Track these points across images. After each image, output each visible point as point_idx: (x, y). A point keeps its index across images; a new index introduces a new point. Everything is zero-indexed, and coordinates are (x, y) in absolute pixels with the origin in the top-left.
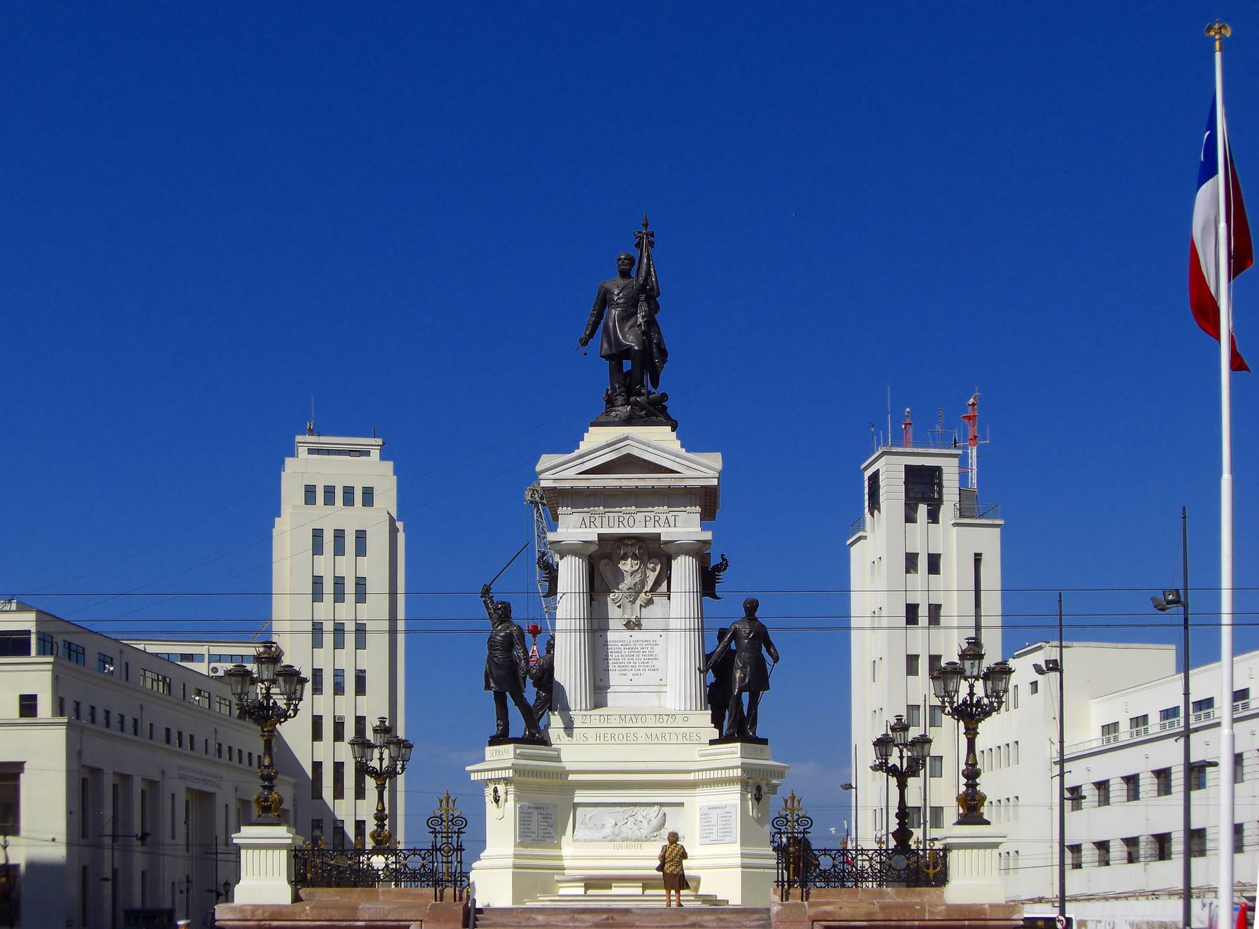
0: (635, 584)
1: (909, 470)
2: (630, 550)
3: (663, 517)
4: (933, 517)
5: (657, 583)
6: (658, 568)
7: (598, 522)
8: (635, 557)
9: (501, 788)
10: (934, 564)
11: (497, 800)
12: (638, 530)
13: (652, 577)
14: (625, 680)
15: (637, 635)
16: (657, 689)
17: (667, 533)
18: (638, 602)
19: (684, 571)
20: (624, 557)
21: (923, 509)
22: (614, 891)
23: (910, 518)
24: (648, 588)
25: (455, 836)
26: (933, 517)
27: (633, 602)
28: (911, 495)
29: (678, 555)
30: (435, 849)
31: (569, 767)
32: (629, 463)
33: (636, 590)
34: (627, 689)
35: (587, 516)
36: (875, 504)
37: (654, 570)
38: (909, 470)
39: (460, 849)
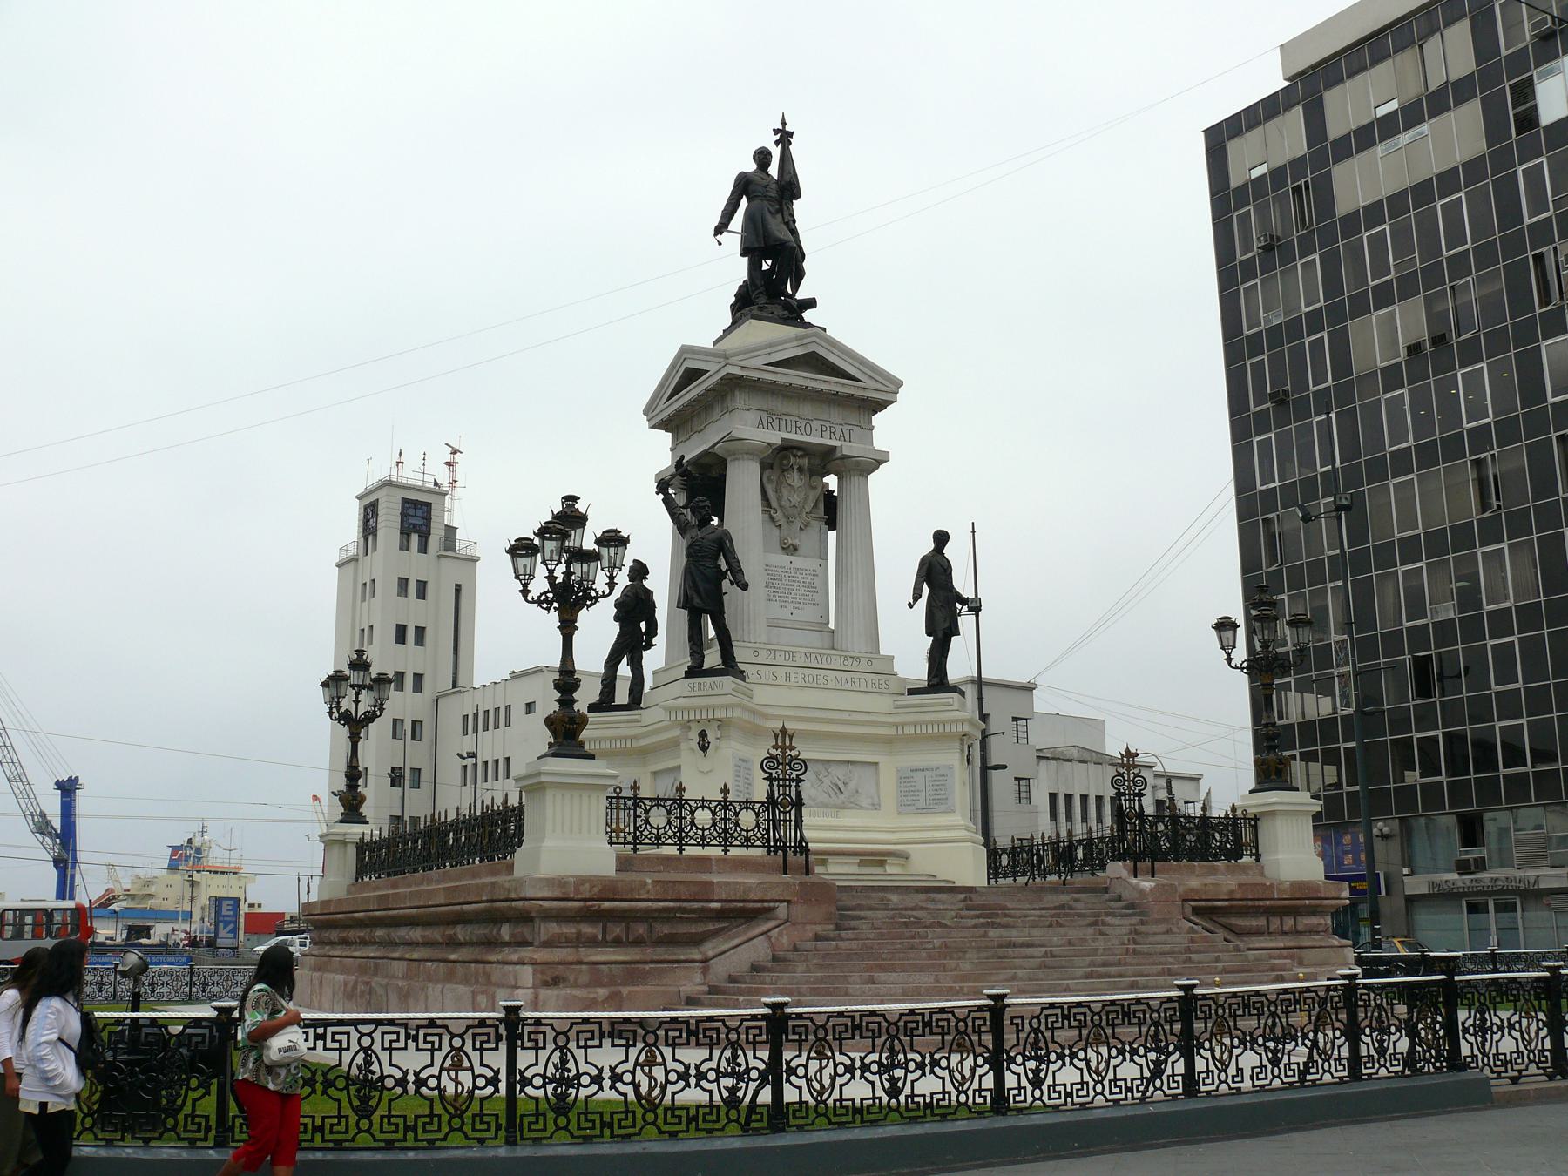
1: (405, 501)
3: (839, 429)
4: (423, 549)
5: (815, 506)
10: (422, 591)
11: (704, 748)
15: (798, 561)
21: (415, 538)
26: (423, 549)
30: (771, 801)
38: (405, 501)
39: (799, 804)
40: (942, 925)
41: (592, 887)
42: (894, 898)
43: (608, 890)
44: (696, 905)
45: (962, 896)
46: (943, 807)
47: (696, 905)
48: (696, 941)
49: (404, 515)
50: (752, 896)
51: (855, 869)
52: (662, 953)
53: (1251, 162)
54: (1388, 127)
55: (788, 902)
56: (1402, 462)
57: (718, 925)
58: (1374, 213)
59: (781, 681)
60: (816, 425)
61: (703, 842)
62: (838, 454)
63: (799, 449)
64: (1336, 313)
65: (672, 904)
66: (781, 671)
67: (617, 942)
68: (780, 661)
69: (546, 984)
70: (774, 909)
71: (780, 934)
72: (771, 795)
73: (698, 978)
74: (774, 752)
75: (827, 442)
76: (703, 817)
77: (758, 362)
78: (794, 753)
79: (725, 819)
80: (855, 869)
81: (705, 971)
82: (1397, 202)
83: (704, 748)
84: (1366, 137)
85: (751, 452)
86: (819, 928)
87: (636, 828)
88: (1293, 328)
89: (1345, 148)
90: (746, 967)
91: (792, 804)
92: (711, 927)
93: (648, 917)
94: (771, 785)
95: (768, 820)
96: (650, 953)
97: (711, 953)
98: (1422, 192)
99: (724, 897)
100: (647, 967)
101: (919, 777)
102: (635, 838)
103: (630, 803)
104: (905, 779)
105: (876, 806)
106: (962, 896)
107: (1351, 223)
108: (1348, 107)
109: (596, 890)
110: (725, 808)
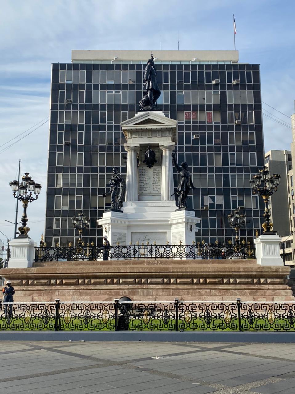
11: (191, 230)
53: (66, 78)
54: (110, 87)
56: (102, 170)
58: (103, 107)
64: (88, 128)
82: (110, 107)
83: (191, 230)
84: (103, 87)
88: (74, 127)
89: (96, 87)
98: (117, 107)
107: (96, 107)
108: (99, 78)
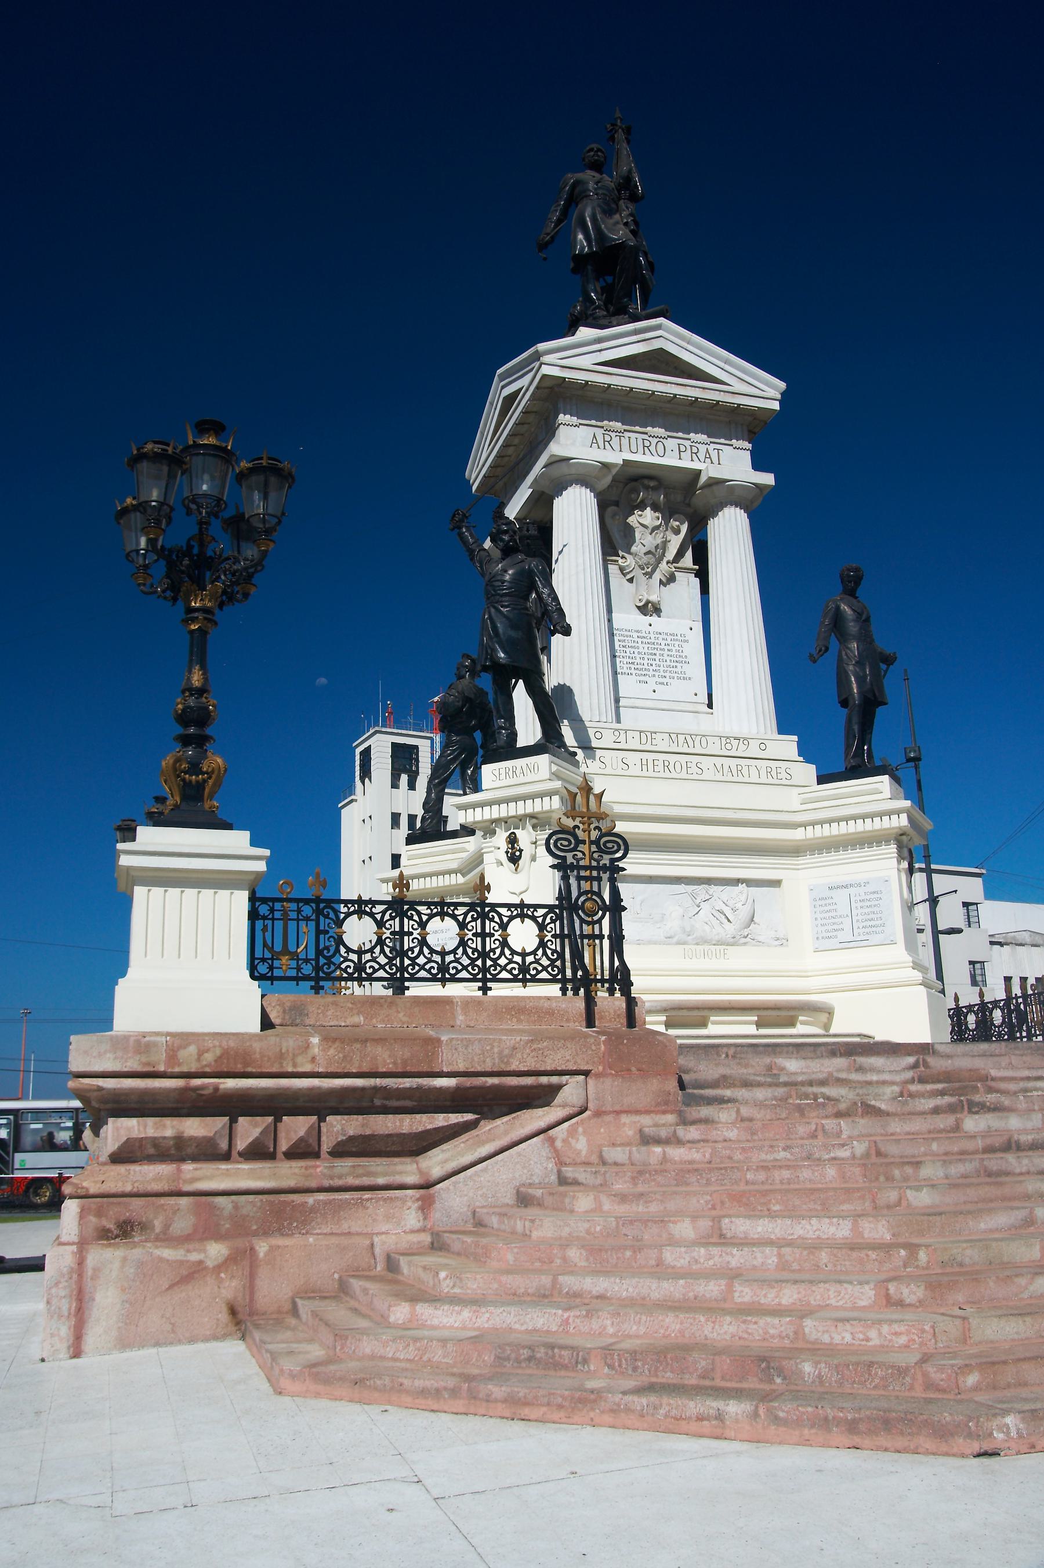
0: (657, 547)
2: (652, 496)
5: (680, 555)
6: (684, 528)
7: (615, 442)
8: (655, 508)
9: (525, 837)
11: (514, 859)
12: (671, 460)
13: (675, 542)
14: (645, 691)
16: (690, 707)
17: (710, 471)
18: (657, 576)
19: (730, 534)
20: (642, 507)
21: (404, 778)
22: (712, 1029)
23: (395, 785)
24: (671, 554)
25: (605, 876)
26: (412, 786)
27: (649, 575)
28: (397, 766)
29: (721, 506)
30: (565, 905)
31: (618, 809)
32: (660, 362)
33: (657, 554)
34: (649, 704)
35: (599, 432)
36: (366, 772)
37: (677, 532)
39: (616, 908)
40: (870, 1110)
41: (200, 1054)
42: (793, 1065)
43: (234, 1058)
44: (407, 1083)
45: (911, 1060)
46: (875, 939)
47: (407, 1083)
48: (419, 1145)
49: (394, 756)
50: (514, 1066)
51: (752, 1030)
52: (346, 1169)
55: (586, 1073)
57: (455, 1118)
59: (635, 770)
60: (672, 444)
61: (443, 975)
62: (703, 479)
63: (651, 478)
65: (359, 1082)
66: (633, 758)
67: (258, 1152)
68: (634, 744)
69: (104, 1235)
70: (559, 1087)
71: (572, 1132)
72: (564, 896)
73: (412, 1218)
74: (569, 823)
75: (686, 463)
76: (443, 933)
77: (586, 362)
78: (604, 826)
79: (483, 935)
80: (752, 1030)
81: (426, 1205)
83: (514, 859)
85: (584, 477)
86: (646, 1120)
87: (319, 952)
90: (508, 1197)
91: (605, 908)
92: (441, 1120)
93: (320, 1106)
94: (565, 878)
95: (561, 936)
96: (321, 1170)
97: (437, 1172)
99: (461, 1067)
100: (310, 1199)
101: (841, 898)
102: (317, 968)
103: (307, 910)
104: (822, 902)
105: (782, 941)
106: (911, 1060)
109: (209, 1057)
110: (484, 917)
